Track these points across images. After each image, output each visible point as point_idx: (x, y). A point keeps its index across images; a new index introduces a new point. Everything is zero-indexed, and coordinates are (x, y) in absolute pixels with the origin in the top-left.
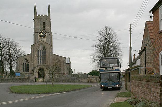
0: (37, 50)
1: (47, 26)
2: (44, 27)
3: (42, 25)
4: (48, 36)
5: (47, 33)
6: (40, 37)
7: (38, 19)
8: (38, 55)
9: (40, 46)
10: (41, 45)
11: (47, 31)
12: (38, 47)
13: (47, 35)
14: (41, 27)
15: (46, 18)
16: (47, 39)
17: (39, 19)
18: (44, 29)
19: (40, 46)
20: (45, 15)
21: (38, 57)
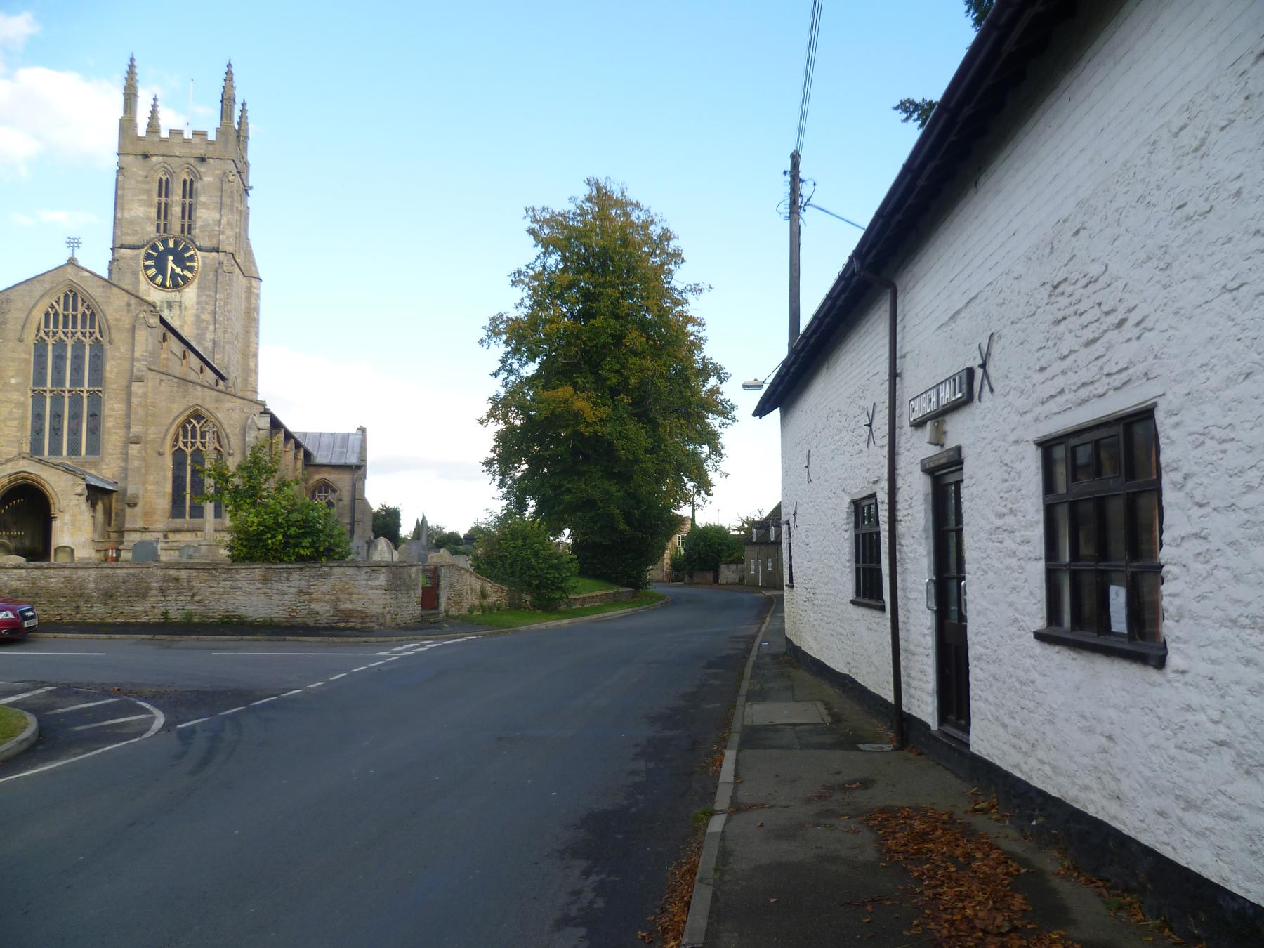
0: (31, 338)
1: (205, 206)
2: (188, 212)
3: (176, 197)
4: (211, 275)
5: (200, 249)
6: (153, 279)
7: (145, 156)
8: (39, 378)
9: (60, 310)
10: (66, 296)
11: (206, 243)
12: (38, 315)
13: (204, 264)
14: (163, 211)
15: (200, 152)
16: (199, 296)
17: (154, 159)
18: (188, 229)
19: (60, 310)
20: (195, 133)
21: (38, 398)
